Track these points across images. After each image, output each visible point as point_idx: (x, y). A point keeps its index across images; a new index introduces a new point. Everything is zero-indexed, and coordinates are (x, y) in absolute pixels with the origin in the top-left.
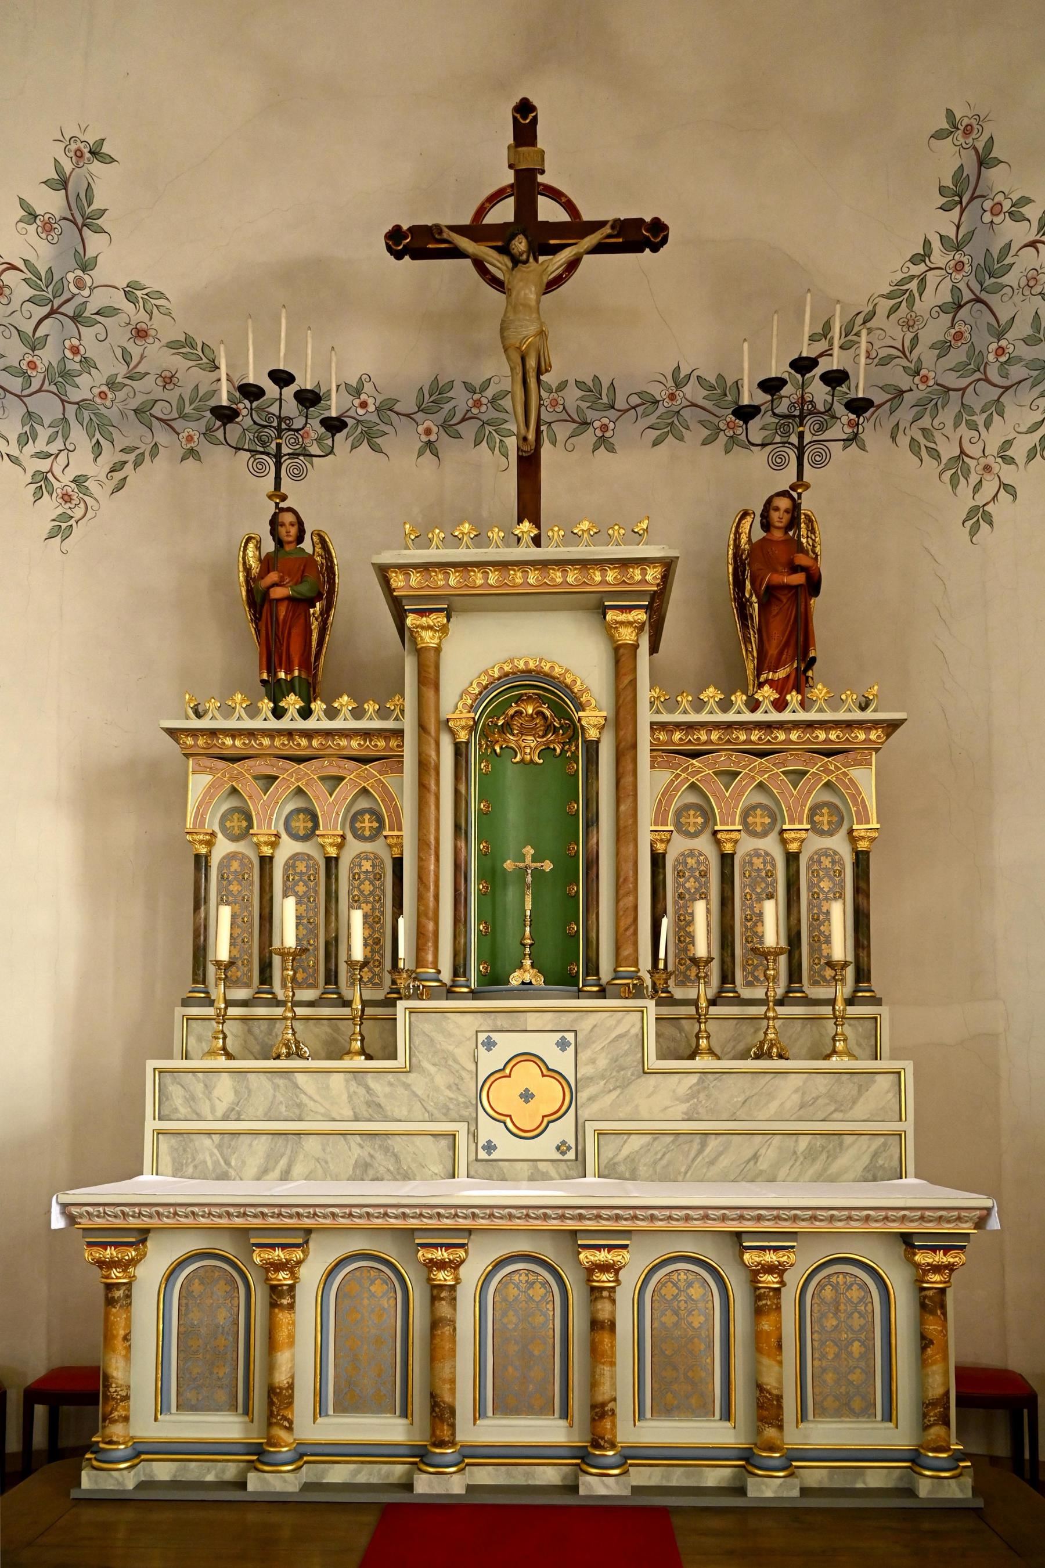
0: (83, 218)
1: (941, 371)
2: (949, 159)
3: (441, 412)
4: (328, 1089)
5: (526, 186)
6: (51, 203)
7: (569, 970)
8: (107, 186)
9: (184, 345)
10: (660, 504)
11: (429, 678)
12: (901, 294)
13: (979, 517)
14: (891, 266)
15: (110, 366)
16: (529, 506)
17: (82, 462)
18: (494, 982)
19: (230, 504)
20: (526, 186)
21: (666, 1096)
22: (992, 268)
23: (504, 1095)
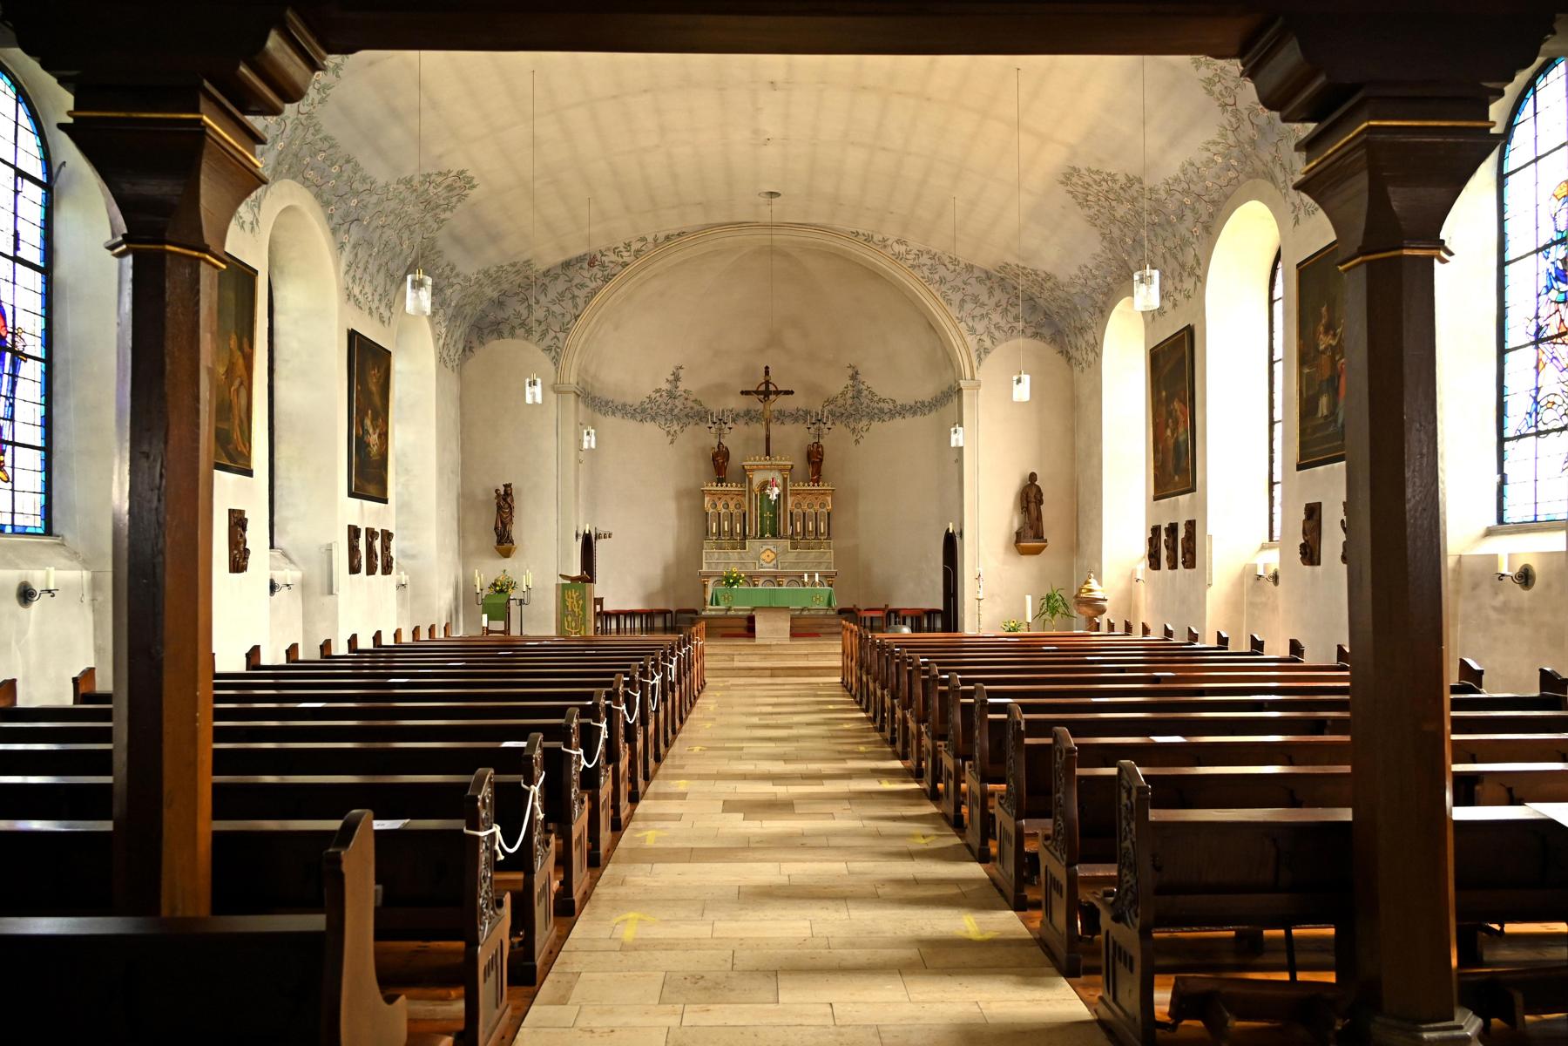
0: (677, 379)
1: (850, 410)
2: (850, 372)
3: (750, 416)
4: (734, 555)
5: (767, 383)
7: (775, 534)
8: (682, 373)
10: (792, 439)
12: (843, 394)
14: (841, 389)
16: (768, 453)
17: (676, 427)
18: (762, 536)
20: (767, 383)
21: (792, 556)
22: (860, 392)
23: (764, 556)
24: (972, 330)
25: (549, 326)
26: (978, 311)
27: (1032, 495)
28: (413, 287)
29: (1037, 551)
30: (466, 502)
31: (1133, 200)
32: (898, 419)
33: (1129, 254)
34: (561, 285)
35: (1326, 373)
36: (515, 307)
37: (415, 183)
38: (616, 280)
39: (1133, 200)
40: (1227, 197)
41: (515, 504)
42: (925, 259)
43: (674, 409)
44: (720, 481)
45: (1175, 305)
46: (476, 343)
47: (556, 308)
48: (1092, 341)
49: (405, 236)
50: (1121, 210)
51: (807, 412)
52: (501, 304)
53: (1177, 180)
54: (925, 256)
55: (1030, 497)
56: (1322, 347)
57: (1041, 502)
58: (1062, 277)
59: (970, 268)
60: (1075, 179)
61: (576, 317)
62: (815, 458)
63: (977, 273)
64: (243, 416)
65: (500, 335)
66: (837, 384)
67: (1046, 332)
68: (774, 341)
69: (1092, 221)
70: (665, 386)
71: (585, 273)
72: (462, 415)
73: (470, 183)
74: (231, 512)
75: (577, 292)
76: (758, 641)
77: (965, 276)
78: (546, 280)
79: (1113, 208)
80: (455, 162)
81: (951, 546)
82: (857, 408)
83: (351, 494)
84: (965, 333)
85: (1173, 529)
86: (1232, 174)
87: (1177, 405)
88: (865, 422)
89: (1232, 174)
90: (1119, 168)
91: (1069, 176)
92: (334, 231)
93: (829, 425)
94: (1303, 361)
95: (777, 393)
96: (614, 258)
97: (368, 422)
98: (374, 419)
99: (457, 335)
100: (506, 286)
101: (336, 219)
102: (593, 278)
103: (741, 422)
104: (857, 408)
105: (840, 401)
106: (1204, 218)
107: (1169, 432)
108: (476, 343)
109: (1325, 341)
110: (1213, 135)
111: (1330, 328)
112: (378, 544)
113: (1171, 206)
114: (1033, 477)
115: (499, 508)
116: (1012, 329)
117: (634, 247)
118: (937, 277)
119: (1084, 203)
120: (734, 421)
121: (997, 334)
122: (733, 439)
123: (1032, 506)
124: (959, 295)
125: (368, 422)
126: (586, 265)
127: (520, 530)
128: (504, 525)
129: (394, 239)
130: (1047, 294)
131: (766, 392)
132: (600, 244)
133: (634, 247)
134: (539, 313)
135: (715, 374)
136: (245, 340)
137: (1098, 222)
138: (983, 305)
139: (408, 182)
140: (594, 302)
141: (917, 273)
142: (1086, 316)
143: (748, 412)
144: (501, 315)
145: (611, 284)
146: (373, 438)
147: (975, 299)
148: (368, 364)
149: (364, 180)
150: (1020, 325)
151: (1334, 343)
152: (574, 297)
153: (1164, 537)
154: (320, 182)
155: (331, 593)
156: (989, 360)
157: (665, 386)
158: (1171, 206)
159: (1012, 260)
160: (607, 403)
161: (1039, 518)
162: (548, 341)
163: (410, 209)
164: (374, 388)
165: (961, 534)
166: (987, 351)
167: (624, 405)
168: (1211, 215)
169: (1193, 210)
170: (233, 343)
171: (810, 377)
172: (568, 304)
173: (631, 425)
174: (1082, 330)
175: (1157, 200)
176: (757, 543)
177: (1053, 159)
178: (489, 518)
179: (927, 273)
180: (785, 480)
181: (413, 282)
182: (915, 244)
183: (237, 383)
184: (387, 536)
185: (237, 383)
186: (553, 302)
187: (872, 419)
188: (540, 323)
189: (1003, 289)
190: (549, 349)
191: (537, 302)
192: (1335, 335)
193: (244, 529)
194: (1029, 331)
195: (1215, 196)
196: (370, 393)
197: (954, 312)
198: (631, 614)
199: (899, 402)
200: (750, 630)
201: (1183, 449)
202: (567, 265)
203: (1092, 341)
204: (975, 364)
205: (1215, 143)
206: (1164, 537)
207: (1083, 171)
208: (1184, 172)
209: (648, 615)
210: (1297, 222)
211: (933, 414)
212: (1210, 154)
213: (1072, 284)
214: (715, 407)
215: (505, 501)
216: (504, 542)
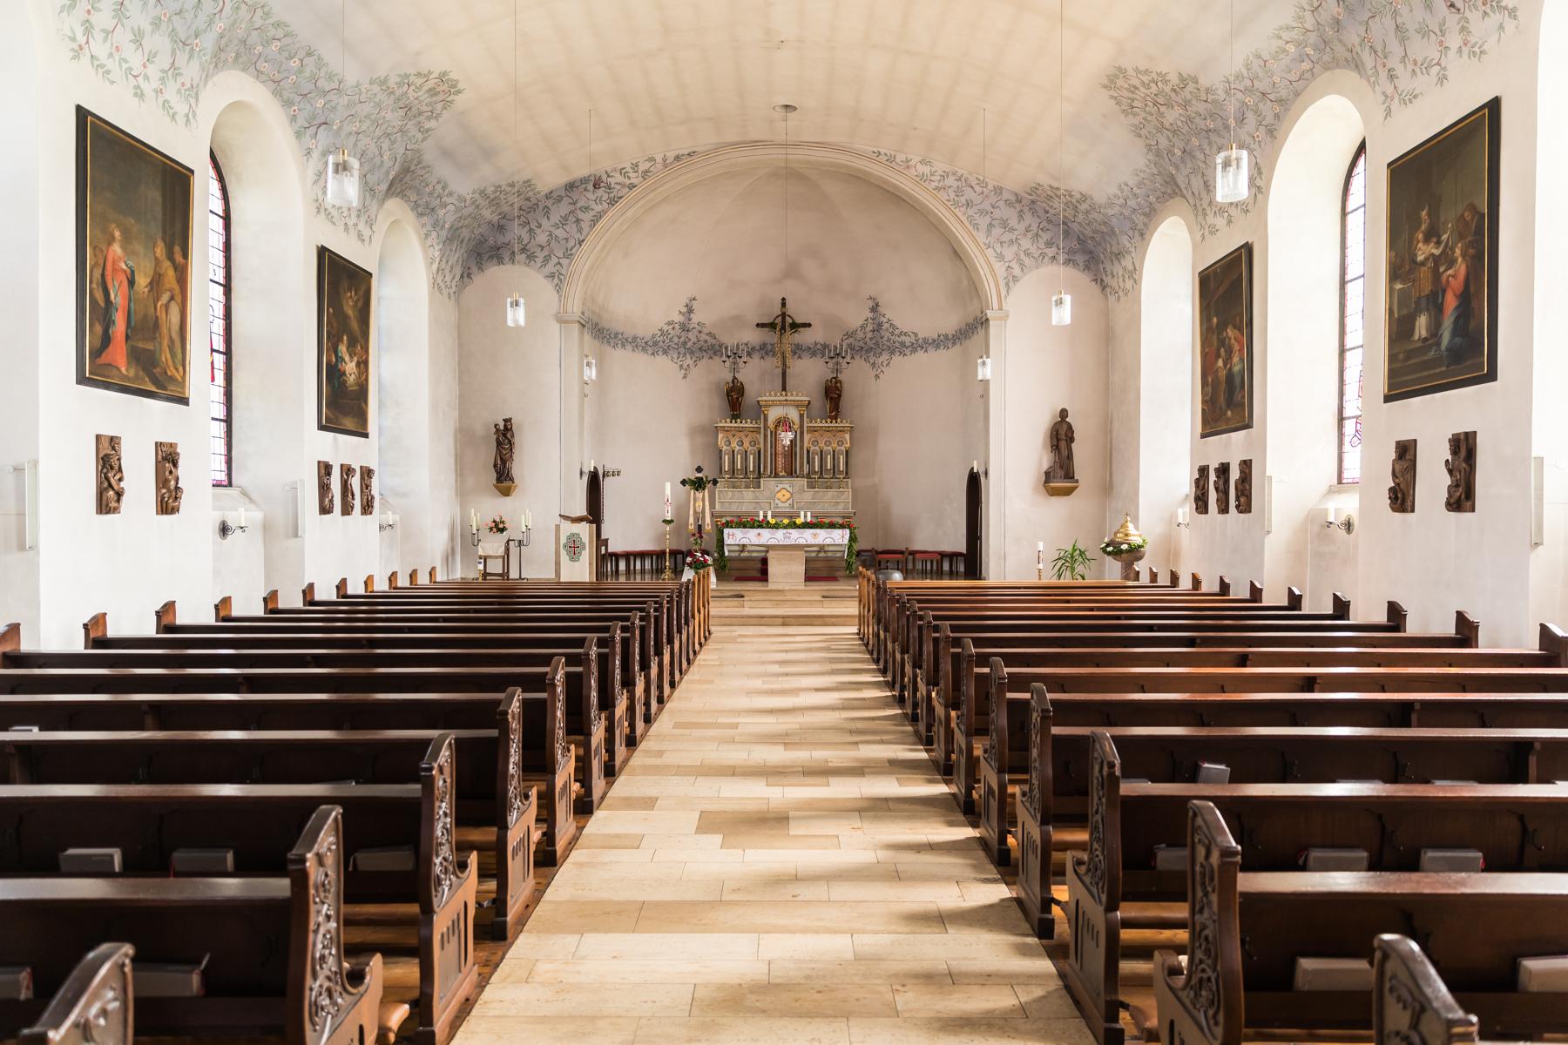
0: (690, 311)
2: (871, 303)
3: (764, 350)
5: (784, 315)
6: (684, 310)
7: (791, 473)
9: (709, 334)
11: (766, 419)
13: (877, 377)
14: (861, 322)
15: (694, 339)
16: (784, 389)
17: (689, 361)
18: (776, 475)
19: (721, 372)
20: (784, 315)
21: (808, 495)
22: (880, 325)
23: (779, 495)
24: (1001, 257)
25: (552, 251)
26: (1007, 237)
27: (1062, 432)
28: (336, 171)
29: (1068, 492)
30: (464, 437)
31: (1185, 105)
32: (920, 354)
33: (1177, 167)
34: (564, 208)
35: (1427, 288)
36: (516, 231)
37: (391, 83)
38: (621, 203)
39: (1185, 105)
40: (1297, 94)
41: (516, 440)
42: (951, 181)
43: (688, 342)
44: (734, 417)
45: (1229, 222)
46: (474, 269)
47: (560, 233)
48: (1130, 267)
49: (385, 146)
50: (1172, 116)
51: (825, 346)
52: (501, 228)
53: (1238, 77)
54: (952, 178)
55: (1061, 436)
56: (1420, 258)
57: (1072, 440)
58: (1099, 197)
59: (998, 190)
60: (1120, 82)
61: (581, 242)
62: (833, 394)
63: (1006, 196)
64: (175, 335)
65: (500, 261)
66: (856, 317)
67: (1081, 259)
68: (791, 271)
69: (1137, 131)
70: (678, 318)
71: (590, 195)
72: (460, 346)
73: (454, 88)
74: (159, 445)
75: (581, 215)
76: (771, 586)
77: (993, 199)
78: (549, 203)
79: (1161, 115)
80: (437, 61)
81: (974, 484)
82: (876, 341)
83: (321, 427)
84: (993, 260)
85: (1224, 470)
86: (1306, 65)
87: (1231, 332)
88: (885, 356)
89: (1306, 65)
90: (1171, 66)
91: (1114, 80)
92: (298, 135)
93: (848, 359)
94: (1395, 273)
95: (795, 326)
96: (619, 178)
97: (343, 348)
98: (352, 345)
99: (453, 260)
100: (505, 208)
101: (301, 122)
102: (598, 201)
103: (756, 357)
104: (876, 341)
105: (860, 335)
106: (1269, 119)
107: (1220, 363)
108: (474, 269)
109: (1424, 251)
110: (1287, 18)
111: (1432, 235)
112: (355, 482)
113: (1231, 108)
114: (1064, 413)
115: (499, 444)
116: (1043, 255)
117: (642, 168)
118: (963, 200)
119: (1130, 110)
120: (749, 354)
121: (1027, 261)
122: (753, 375)
123: (1063, 444)
124: (987, 219)
125: (343, 348)
126: (590, 187)
127: (520, 467)
128: (504, 462)
129: (373, 149)
130: (1081, 217)
131: (782, 324)
132: (601, 166)
133: (642, 168)
134: (542, 238)
135: (732, 306)
136: (177, 249)
137: (1143, 132)
138: (1012, 230)
139: (383, 82)
140: (599, 226)
141: (943, 195)
142: (1124, 240)
143: (763, 347)
144: (501, 239)
145: (618, 206)
146: (350, 367)
147: (1004, 224)
148: (342, 288)
149: (330, 77)
150: (1051, 252)
151: (1437, 252)
152: (578, 221)
153: (1212, 477)
154: (278, 77)
155: (296, 535)
156: (1017, 289)
157: (678, 318)
158: (1231, 108)
159: (1045, 181)
160: (616, 334)
161: (1070, 457)
162: (550, 268)
163: (389, 116)
164: (350, 312)
165: (986, 473)
166: (1015, 279)
167: (635, 338)
168: (1277, 116)
169: (1257, 112)
170: (160, 250)
171: (830, 311)
172: (572, 227)
173: (641, 360)
174: (1118, 256)
175: (1214, 101)
176: (772, 482)
177: (1096, 59)
178: (488, 453)
179: (952, 195)
180: (801, 416)
181: (337, 165)
182: (940, 167)
183: (165, 297)
184: (367, 473)
185: (165, 297)
186: (556, 226)
187: (892, 353)
188: (542, 248)
189: (1034, 213)
190: (552, 276)
191: (540, 226)
192: (1438, 243)
193: (175, 465)
194: (1061, 258)
195: (1283, 93)
196: (346, 317)
197: (981, 237)
198: (642, 555)
199: (920, 336)
200: (763, 575)
201: (1237, 381)
202: (571, 186)
203: (1130, 267)
204: (1003, 293)
205: (1288, 28)
206: (1212, 477)
207: (1131, 72)
208: (1248, 67)
209: (660, 555)
210: (1388, 113)
211: (958, 347)
212: (1281, 43)
213: (1111, 205)
214: (730, 340)
215: (505, 437)
216: (503, 478)
